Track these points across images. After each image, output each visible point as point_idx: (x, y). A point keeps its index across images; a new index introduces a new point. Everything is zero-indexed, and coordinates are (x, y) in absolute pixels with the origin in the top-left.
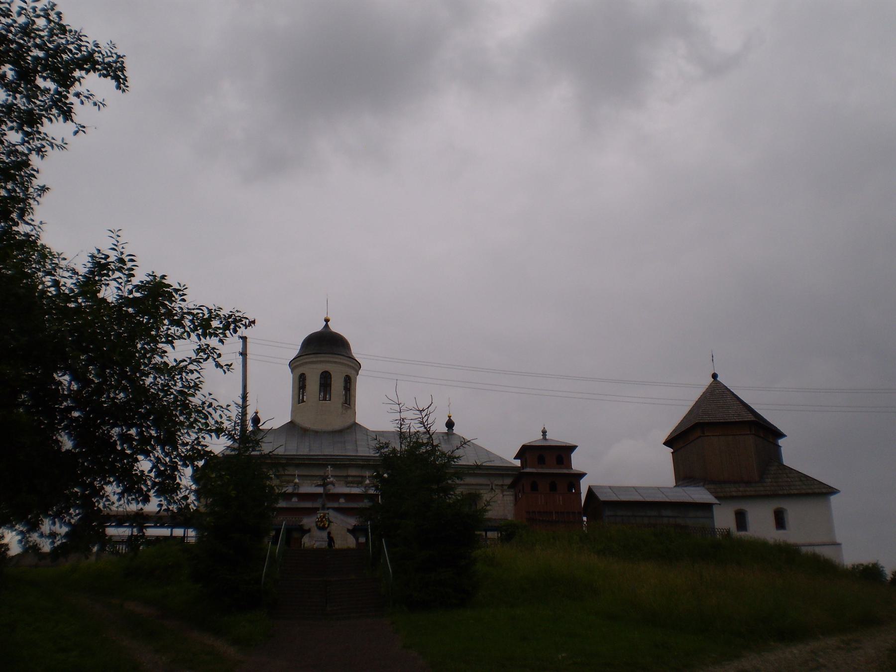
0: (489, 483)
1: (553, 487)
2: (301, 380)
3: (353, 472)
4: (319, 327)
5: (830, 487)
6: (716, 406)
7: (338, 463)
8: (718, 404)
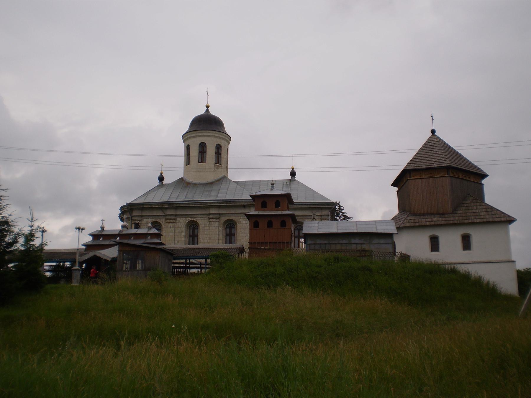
0: (312, 214)
1: (270, 224)
2: (188, 149)
3: (213, 211)
4: (202, 111)
5: (509, 216)
6: (424, 155)
7: (202, 205)
8: (427, 153)
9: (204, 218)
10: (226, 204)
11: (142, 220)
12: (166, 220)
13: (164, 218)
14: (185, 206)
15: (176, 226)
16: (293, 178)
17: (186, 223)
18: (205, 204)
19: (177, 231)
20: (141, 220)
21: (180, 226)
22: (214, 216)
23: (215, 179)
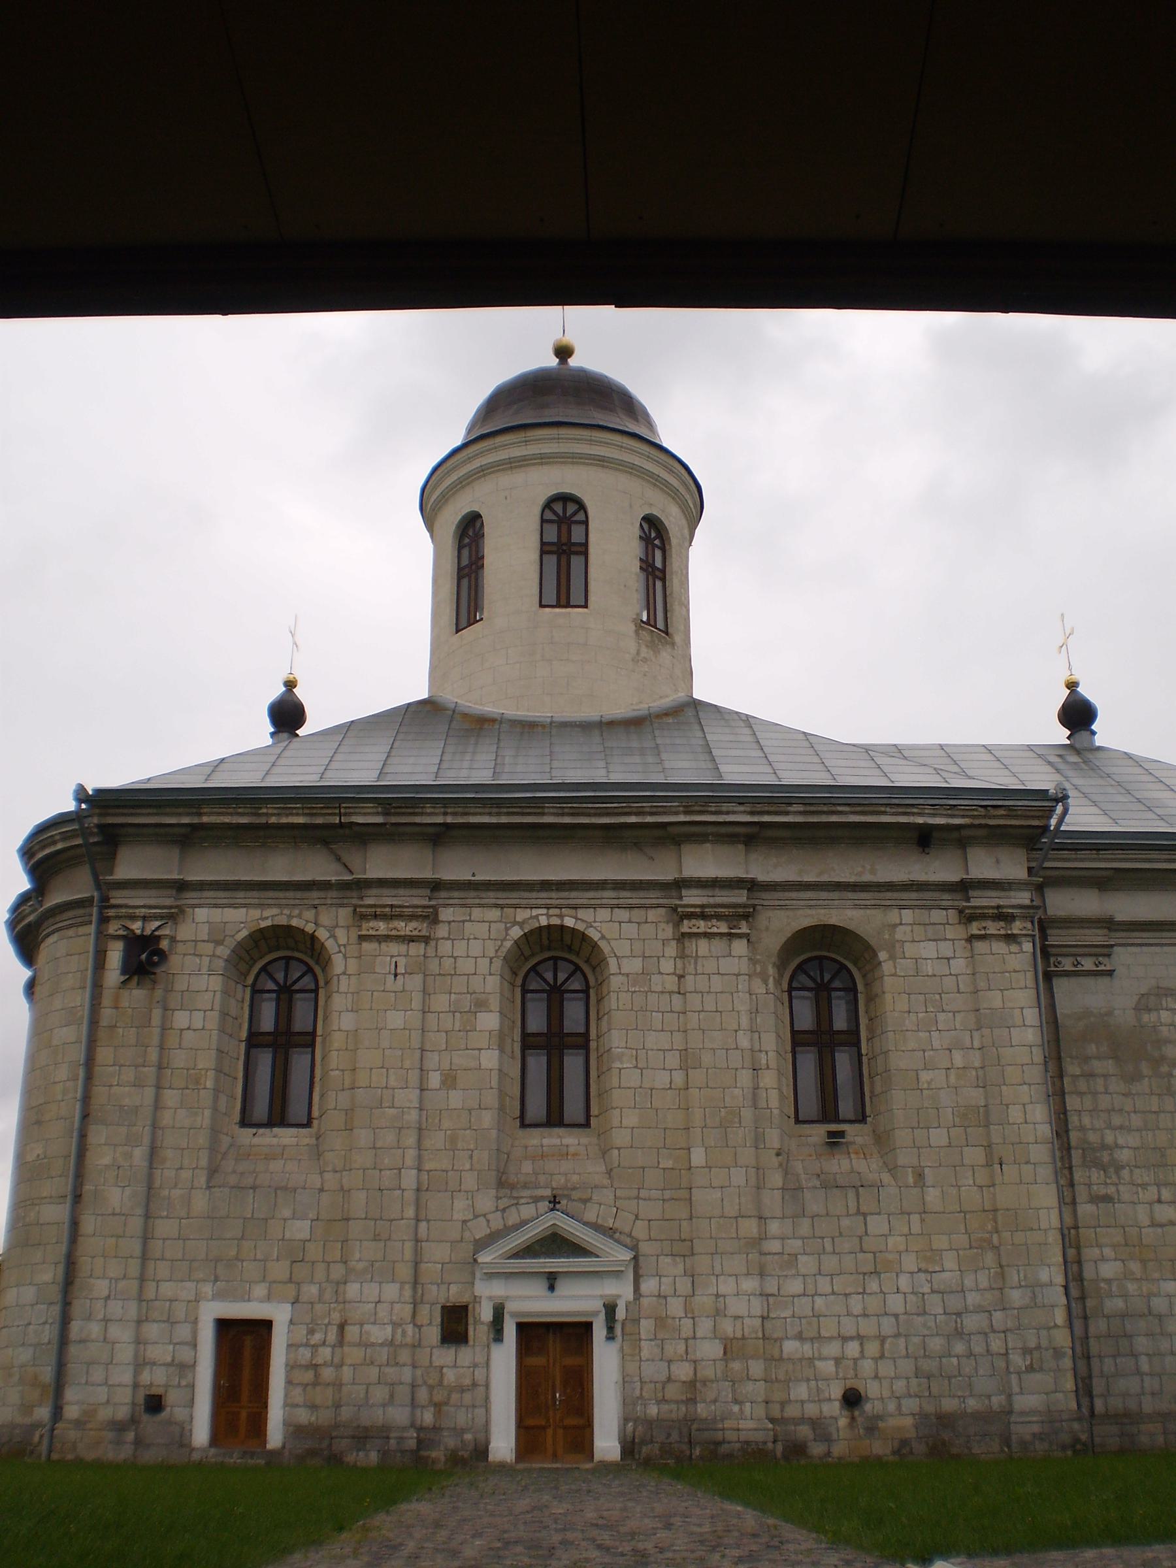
2: (467, 541)
7: (633, 819)
9: (638, 914)
10: (799, 819)
11: (181, 910)
12: (361, 917)
13: (342, 905)
14: (504, 820)
15: (433, 966)
16: (1084, 734)
17: (508, 944)
18: (652, 814)
19: (441, 1002)
20: (173, 916)
21: (466, 966)
22: (719, 900)
23: (646, 706)
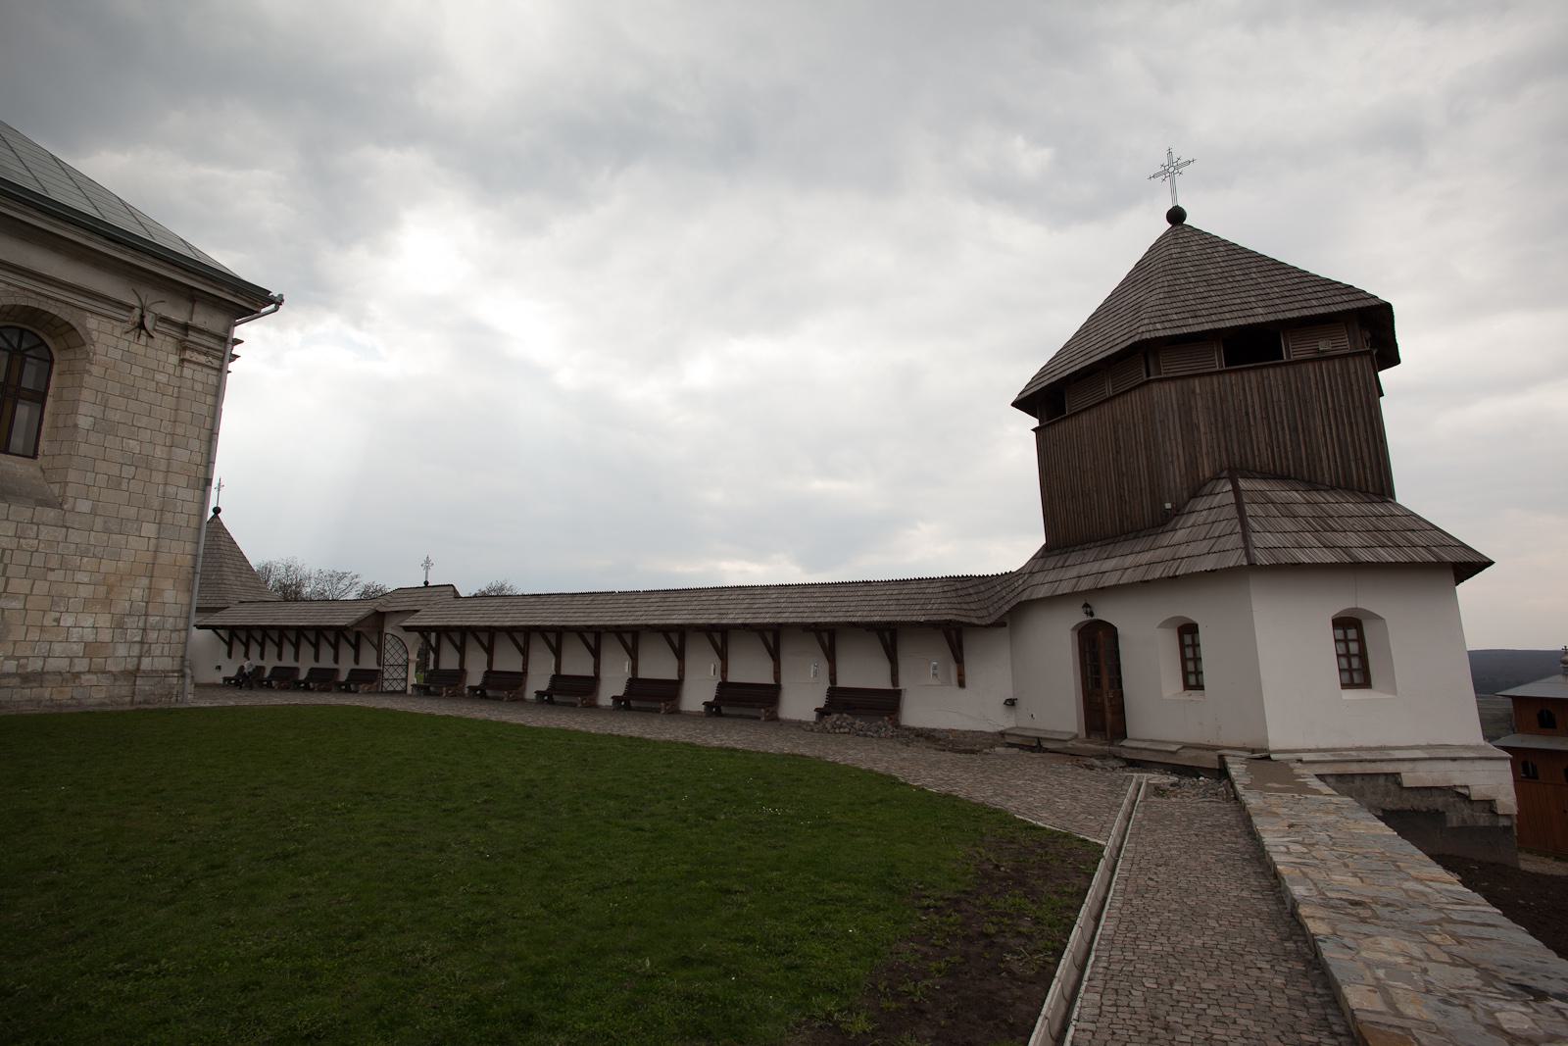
0: (133, 301)
